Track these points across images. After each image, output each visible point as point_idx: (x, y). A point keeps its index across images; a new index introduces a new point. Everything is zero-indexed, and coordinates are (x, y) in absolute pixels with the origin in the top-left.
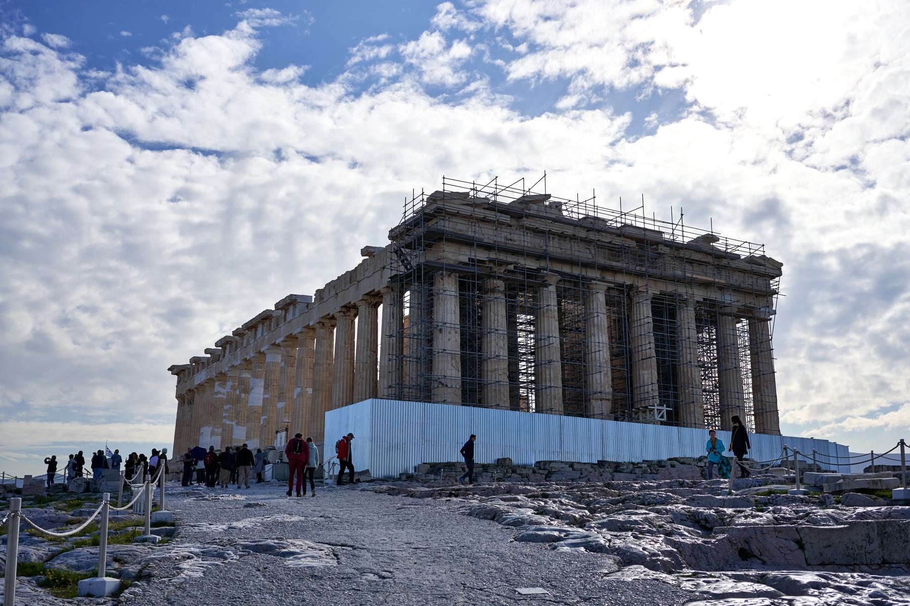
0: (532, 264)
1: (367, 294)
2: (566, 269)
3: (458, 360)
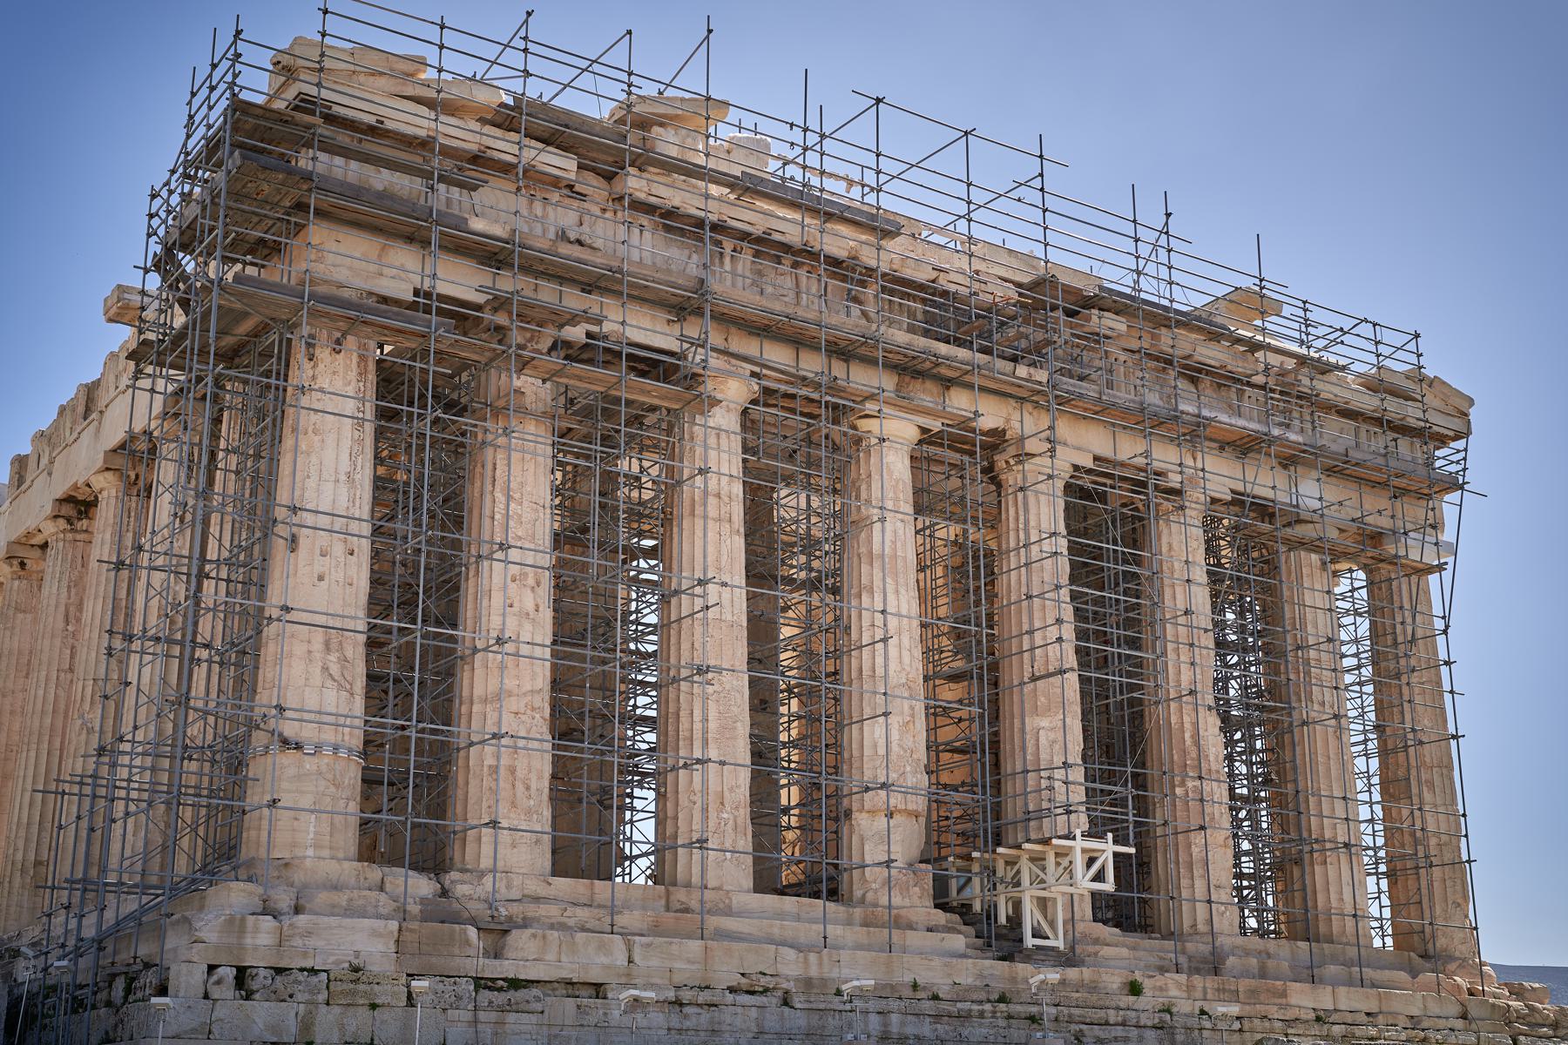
0: (648, 330)
2: (778, 355)
3: (355, 649)
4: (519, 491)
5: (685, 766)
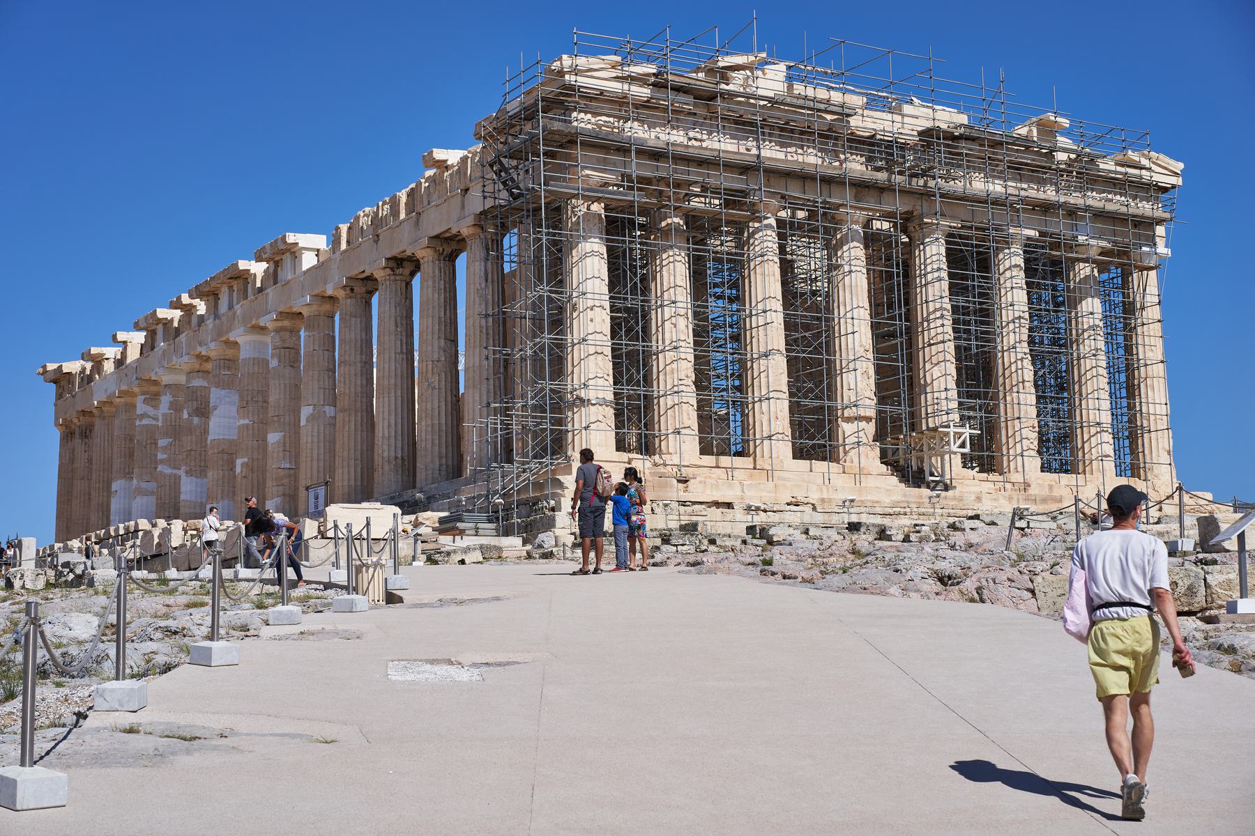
1: (437, 237)
4: (674, 273)
5: (760, 401)
